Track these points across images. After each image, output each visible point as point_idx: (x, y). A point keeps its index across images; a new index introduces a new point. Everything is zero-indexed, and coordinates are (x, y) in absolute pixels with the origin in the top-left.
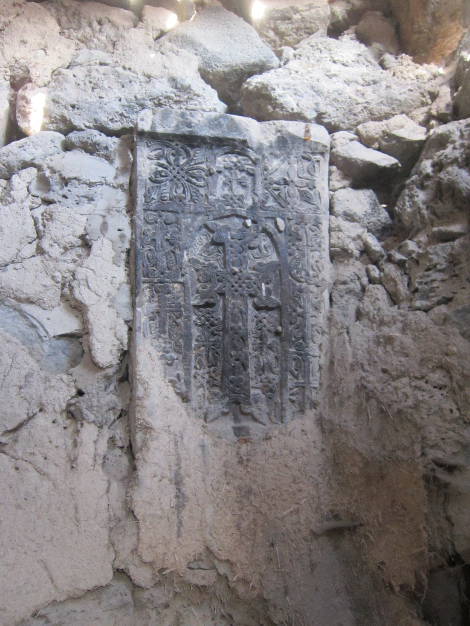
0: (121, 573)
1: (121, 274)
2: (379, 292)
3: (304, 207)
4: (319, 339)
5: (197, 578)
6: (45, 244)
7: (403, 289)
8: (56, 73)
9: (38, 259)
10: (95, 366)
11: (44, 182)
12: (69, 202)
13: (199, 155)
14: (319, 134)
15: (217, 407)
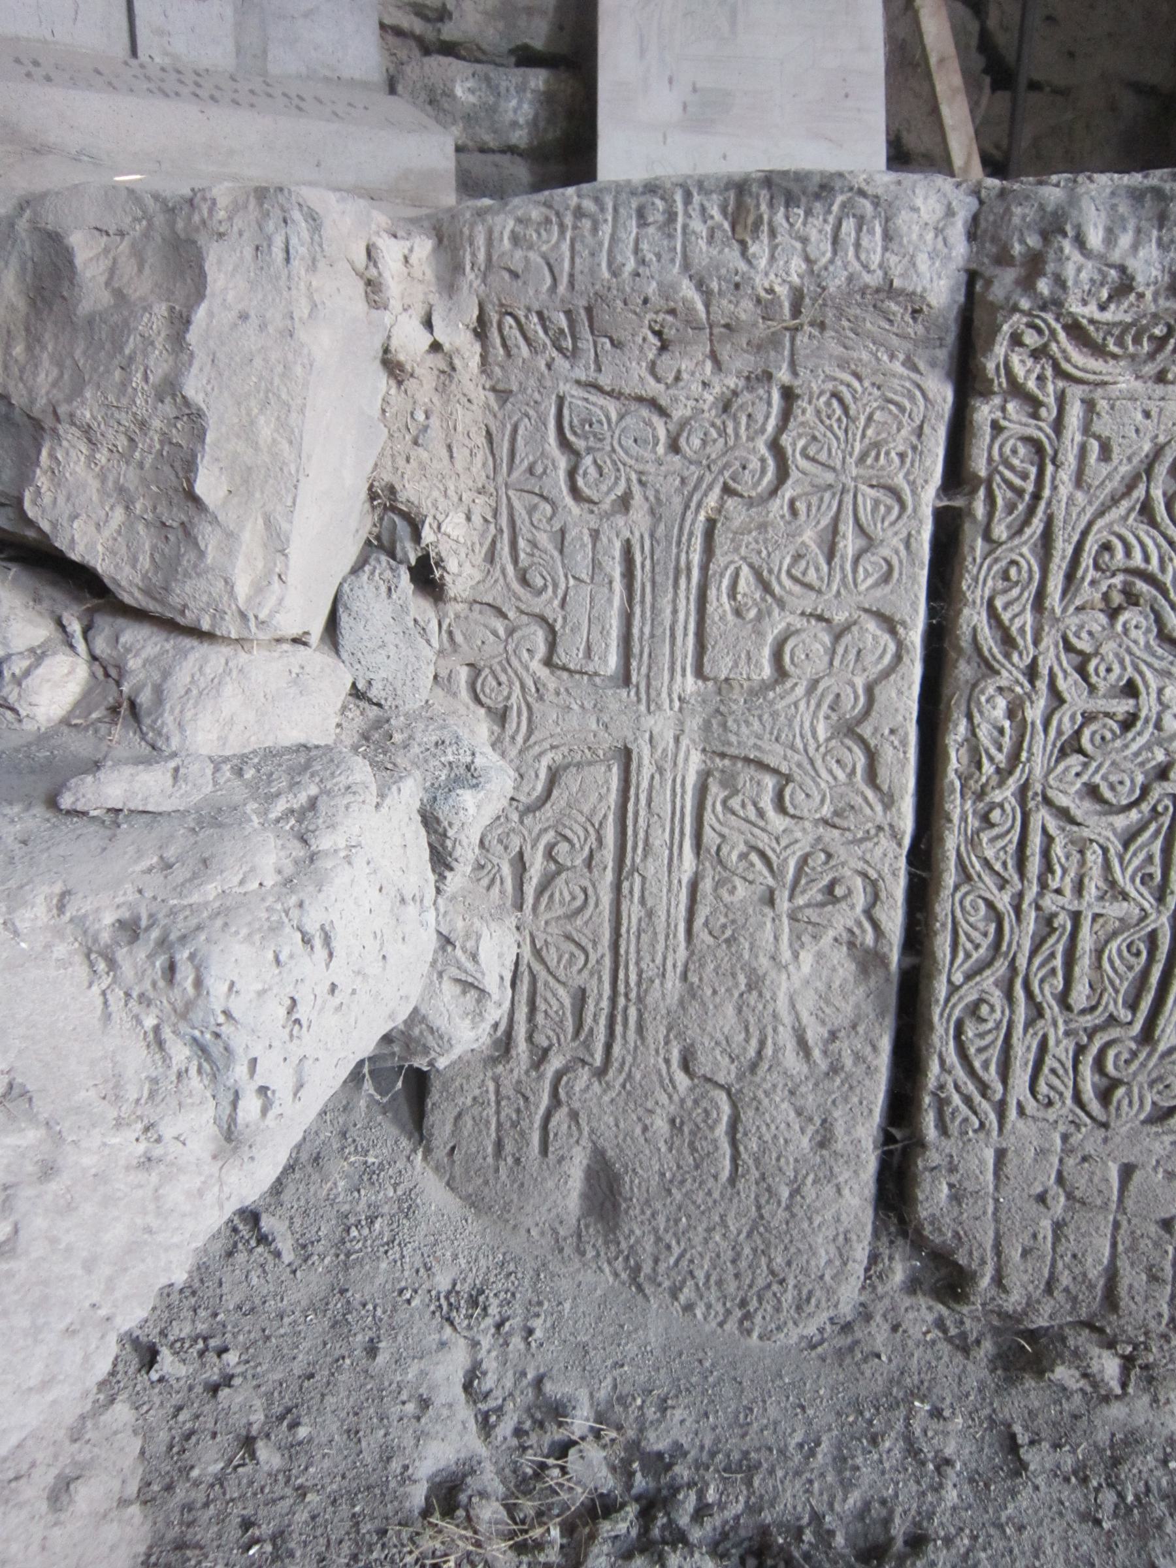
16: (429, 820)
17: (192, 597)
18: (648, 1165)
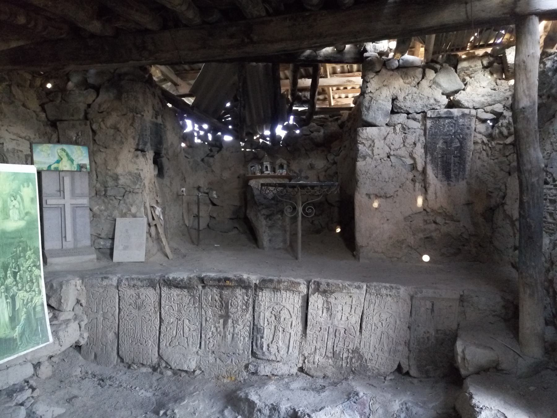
0: (424, 210)
1: (423, 151)
2: (484, 153)
3: (468, 131)
4: (469, 164)
5: (439, 211)
6: (406, 144)
7: (490, 154)
8: (405, 98)
9: (404, 148)
10: (417, 170)
11: (404, 129)
12: (410, 133)
13: (441, 120)
14: (473, 112)
15: (444, 179)
16: (79, 324)
17: (60, 309)
18: (99, 354)
